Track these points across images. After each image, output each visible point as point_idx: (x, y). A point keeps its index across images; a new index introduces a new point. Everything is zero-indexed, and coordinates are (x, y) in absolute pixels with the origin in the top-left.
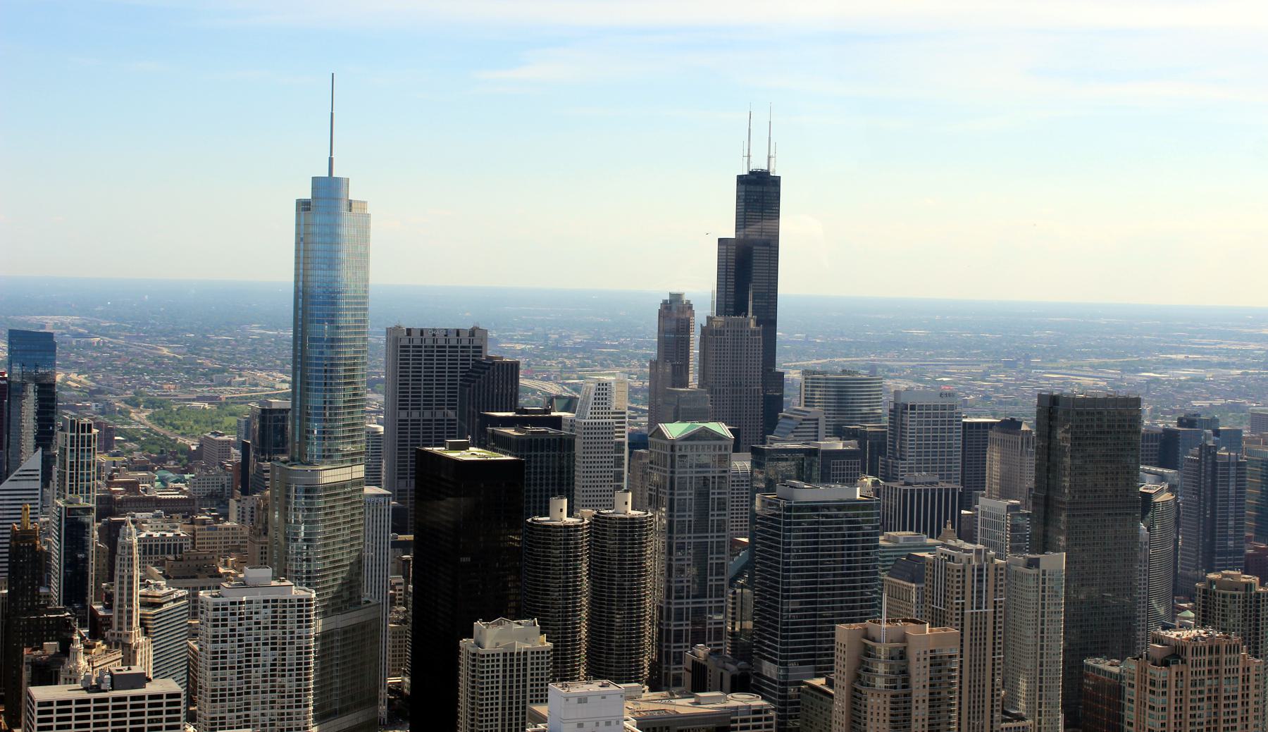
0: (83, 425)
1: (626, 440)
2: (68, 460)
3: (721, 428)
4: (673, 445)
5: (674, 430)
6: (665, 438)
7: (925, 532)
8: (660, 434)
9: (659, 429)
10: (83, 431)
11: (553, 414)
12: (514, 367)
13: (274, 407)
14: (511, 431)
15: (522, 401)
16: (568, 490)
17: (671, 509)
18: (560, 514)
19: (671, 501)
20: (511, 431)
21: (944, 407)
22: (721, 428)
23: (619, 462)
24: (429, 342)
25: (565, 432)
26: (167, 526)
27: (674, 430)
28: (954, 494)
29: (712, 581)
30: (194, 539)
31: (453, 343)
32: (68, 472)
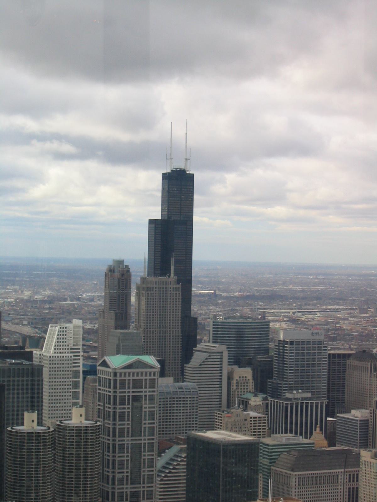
1: (81, 369)
3: (151, 360)
5: (117, 361)
6: (109, 367)
7: (301, 434)
8: (105, 364)
9: (104, 361)
16: (38, 406)
18: (29, 423)
21: (314, 343)
22: (151, 360)
27: (117, 361)
28: (322, 407)
29: (145, 471)
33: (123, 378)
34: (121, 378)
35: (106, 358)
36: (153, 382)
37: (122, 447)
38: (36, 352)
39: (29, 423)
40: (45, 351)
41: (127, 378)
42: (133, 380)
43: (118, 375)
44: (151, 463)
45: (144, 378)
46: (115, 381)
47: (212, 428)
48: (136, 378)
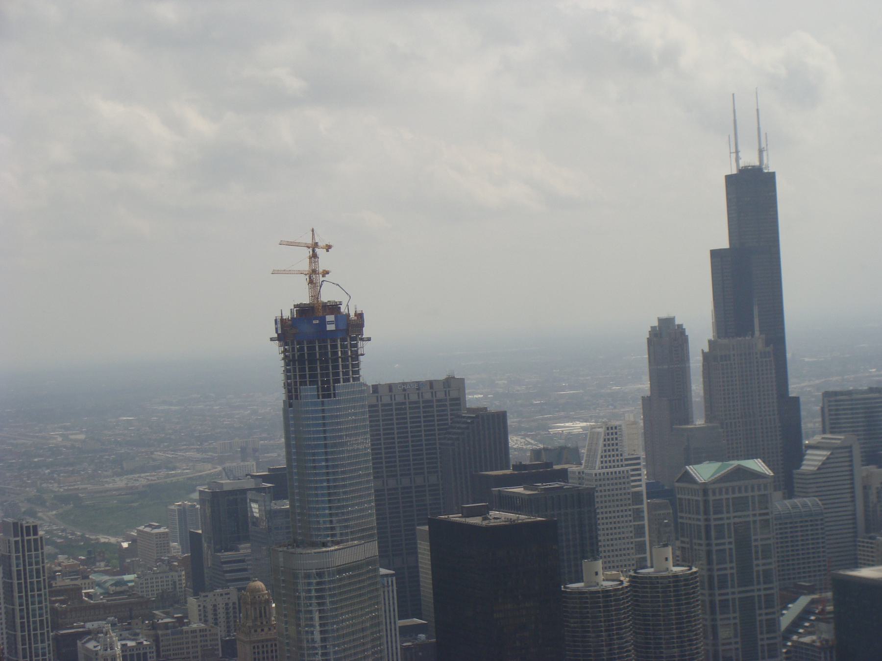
0: (28, 528)
1: (643, 489)
2: (14, 569)
3: (757, 465)
4: (705, 489)
5: (704, 472)
8: (687, 478)
9: (687, 473)
10: (28, 534)
11: (556, 467)
12: (500, 418)
13: (226, 488)
14: (519, 490)
15: (514, 457)
17: (709, 562)
19: (709, 553)
20: (519, 490)
22: (757, 465)
23: (638, 515)
24: (400, 399)
25: (572, 483)
26: (126, 634)
27: (704, 472)
30: (158, 647)
31: (427, 396)
32: (15, 582)
33: (718, 497)
34: (714, 498)
35: (691, 469)
36: (765, 500)
37: (724, 604)
38: (573, 468)
39: (602, 577)
40: (586, 467)
41: (724, 496)
42: (733, 498)
43: (710, 493)
44: (772, 625)
45: (750, 494)
46: (706, 502)
47: (856, 565)
48: (737, 495)
